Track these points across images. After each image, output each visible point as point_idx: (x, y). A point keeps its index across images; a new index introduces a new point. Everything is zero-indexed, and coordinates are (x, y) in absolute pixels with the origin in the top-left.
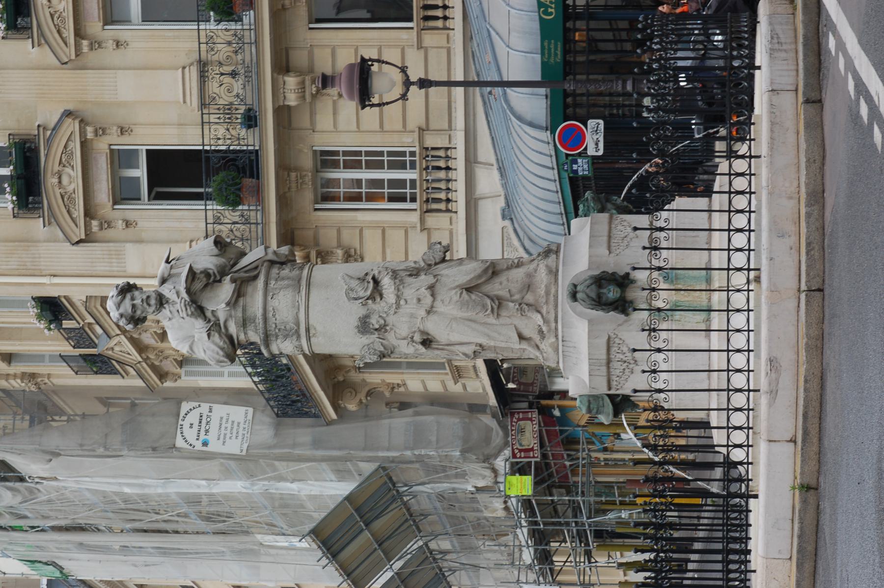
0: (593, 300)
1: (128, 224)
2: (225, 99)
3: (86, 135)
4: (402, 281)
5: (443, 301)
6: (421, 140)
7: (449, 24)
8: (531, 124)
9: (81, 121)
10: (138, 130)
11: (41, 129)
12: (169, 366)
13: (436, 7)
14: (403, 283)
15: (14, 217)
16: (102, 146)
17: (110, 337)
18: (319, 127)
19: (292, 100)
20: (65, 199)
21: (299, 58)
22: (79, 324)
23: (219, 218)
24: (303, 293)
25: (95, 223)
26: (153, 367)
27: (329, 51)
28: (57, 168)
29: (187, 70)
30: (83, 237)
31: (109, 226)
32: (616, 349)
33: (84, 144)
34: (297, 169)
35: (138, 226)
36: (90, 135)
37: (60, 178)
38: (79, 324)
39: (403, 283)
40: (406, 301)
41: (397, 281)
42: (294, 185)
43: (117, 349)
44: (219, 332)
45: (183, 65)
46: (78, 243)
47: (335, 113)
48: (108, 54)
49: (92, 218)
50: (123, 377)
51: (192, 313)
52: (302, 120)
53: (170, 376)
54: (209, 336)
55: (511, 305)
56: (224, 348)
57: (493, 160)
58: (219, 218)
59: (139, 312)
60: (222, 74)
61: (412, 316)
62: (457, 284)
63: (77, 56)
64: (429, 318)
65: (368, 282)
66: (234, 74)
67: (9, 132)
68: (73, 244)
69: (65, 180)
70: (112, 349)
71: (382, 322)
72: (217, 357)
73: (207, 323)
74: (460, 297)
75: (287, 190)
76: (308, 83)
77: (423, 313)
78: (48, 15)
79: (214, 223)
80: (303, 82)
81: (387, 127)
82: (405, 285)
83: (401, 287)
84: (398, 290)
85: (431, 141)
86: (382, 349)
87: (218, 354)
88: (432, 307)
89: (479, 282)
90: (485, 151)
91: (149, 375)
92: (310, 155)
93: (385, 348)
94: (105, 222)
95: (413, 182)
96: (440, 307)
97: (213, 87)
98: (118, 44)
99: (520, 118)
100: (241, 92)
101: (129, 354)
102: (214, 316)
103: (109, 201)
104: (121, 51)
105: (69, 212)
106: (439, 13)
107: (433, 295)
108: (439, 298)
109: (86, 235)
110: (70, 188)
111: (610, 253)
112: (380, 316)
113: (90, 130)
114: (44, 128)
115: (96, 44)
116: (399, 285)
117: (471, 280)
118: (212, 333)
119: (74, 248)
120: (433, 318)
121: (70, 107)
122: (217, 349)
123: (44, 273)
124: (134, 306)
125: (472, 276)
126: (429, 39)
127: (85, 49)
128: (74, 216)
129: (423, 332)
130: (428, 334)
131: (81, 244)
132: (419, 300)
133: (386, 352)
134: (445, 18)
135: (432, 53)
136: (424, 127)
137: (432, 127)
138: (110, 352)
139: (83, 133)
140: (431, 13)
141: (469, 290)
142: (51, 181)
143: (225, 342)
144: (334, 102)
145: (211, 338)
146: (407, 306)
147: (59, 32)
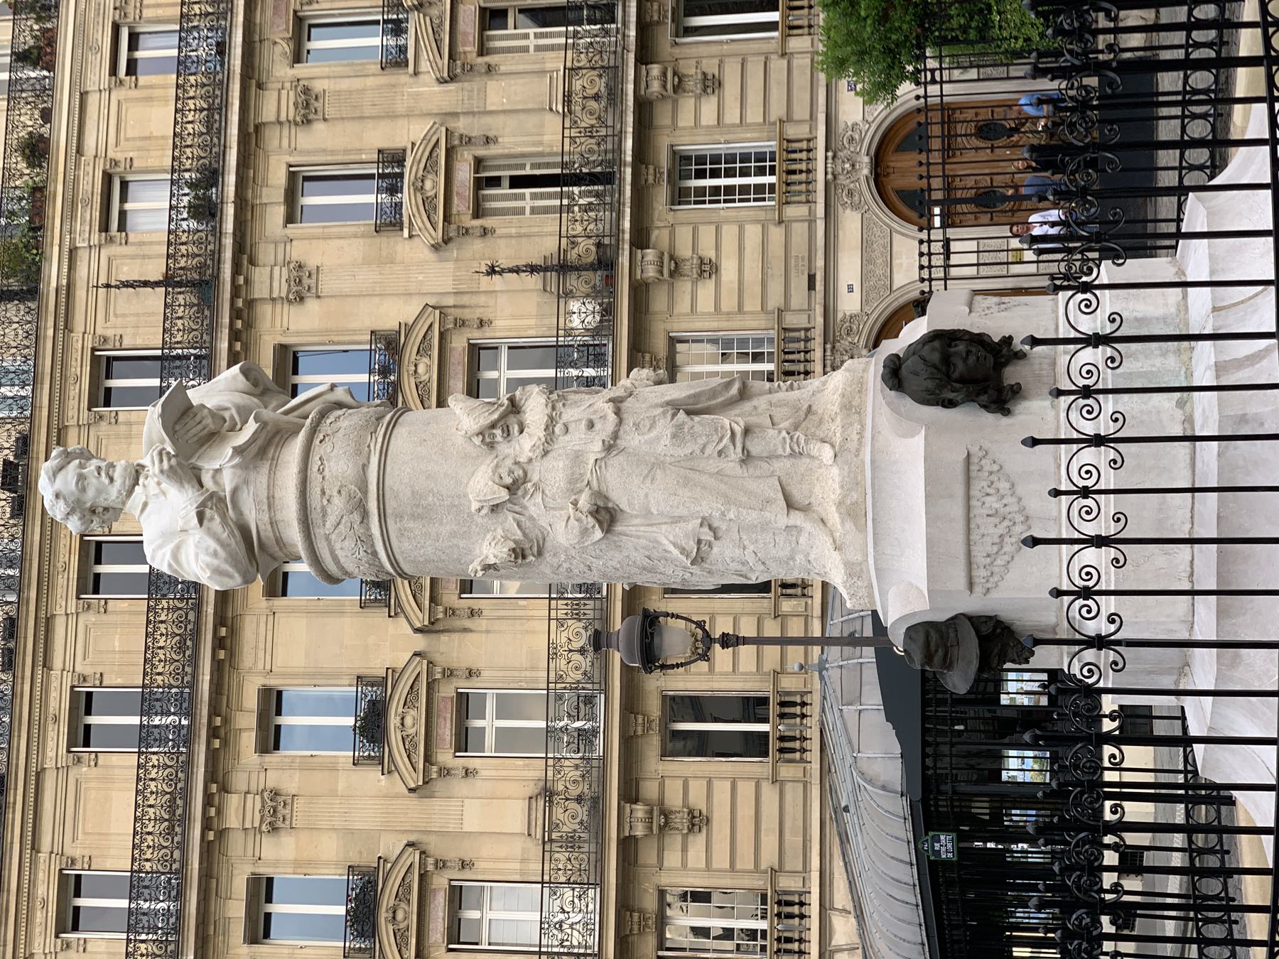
0: (934, 366)
2: (569, 826)
3: (426, 866)
5: (637, 425)
6: (773, 882)
7: (807, 756)
8: (884, 788)
9: (423, 853)
10: (480, 865)
11: (382, 861)
13: (793, 739)
16: (440, 882)
18: (666, 864)
19: (639, 831)
21: (650, 789)
27: (680, 783)
28: (392, 903)
29: (533, 801)
32: (985, 484)
33: (423, 877)
34: (641, 911)
36: (430, 868)
37: (394, 912)
42: (636, 927)
44: (224, 517)
45: (529, 794)
47: (684, 850)
48: (459, 786)
51: (171, 467)
52: (648, 855)
54: (201, 517)
55: (772, 432)
56: (229, 545)
57: (850, 907)
59: (91, 493)
60: (567, 799)
61: (577, 457)
62: (668, 398)
63: (425, 783)
64: (610, 462)
66: (579, 799)
67: (350, 864)
69: (400, 915)
72: (216, 562)
73: (202, 494)
74: (672, 419)
75: (628, 932)
76: (656, 813)
78: (400, 738)
80: (651, 812)
81: (739, 866)
84: (554, 408)
85: (786, 883)
87: (215, 554)
88: (615, 436)
90: (841, 897)
92: (656, 894)
93: (525, 534)
95: (764, 932)
96: (631, 439)
97: (559, 813)
98: (467, 773)
99: (870, 782)
100: (585, 818)
102: (216, 482)
104: (470, 780)
105: (399, 951)
106: (797, 745)
107: (618, 412)
108: (629, 421)
110: (402, 926)
111: (970, 311)
112: (516, 463)
113: (431, 861)
114: (385, 861)
115: (445, 772)
118: (208, 512)
120: (616, 461)
121: (412, 838)
122: (213, 545)
124: (81, 478)
126: (786, 771)
127: (434, 776)
129: (599, 495)
130: (607, 498)
132: (591, 425)
133: (527, 546)
134: (803, 750)
135: (788, 786)
136: (777, 868)
137: (788, 867)
139: (422, 864)
140: (787, 745)
141: (689, 413)
142: (383, 915)
143: (232, 532)
144: (685, 837)
145: (205, 522)
146: (567, 438)
147: (409, 756)
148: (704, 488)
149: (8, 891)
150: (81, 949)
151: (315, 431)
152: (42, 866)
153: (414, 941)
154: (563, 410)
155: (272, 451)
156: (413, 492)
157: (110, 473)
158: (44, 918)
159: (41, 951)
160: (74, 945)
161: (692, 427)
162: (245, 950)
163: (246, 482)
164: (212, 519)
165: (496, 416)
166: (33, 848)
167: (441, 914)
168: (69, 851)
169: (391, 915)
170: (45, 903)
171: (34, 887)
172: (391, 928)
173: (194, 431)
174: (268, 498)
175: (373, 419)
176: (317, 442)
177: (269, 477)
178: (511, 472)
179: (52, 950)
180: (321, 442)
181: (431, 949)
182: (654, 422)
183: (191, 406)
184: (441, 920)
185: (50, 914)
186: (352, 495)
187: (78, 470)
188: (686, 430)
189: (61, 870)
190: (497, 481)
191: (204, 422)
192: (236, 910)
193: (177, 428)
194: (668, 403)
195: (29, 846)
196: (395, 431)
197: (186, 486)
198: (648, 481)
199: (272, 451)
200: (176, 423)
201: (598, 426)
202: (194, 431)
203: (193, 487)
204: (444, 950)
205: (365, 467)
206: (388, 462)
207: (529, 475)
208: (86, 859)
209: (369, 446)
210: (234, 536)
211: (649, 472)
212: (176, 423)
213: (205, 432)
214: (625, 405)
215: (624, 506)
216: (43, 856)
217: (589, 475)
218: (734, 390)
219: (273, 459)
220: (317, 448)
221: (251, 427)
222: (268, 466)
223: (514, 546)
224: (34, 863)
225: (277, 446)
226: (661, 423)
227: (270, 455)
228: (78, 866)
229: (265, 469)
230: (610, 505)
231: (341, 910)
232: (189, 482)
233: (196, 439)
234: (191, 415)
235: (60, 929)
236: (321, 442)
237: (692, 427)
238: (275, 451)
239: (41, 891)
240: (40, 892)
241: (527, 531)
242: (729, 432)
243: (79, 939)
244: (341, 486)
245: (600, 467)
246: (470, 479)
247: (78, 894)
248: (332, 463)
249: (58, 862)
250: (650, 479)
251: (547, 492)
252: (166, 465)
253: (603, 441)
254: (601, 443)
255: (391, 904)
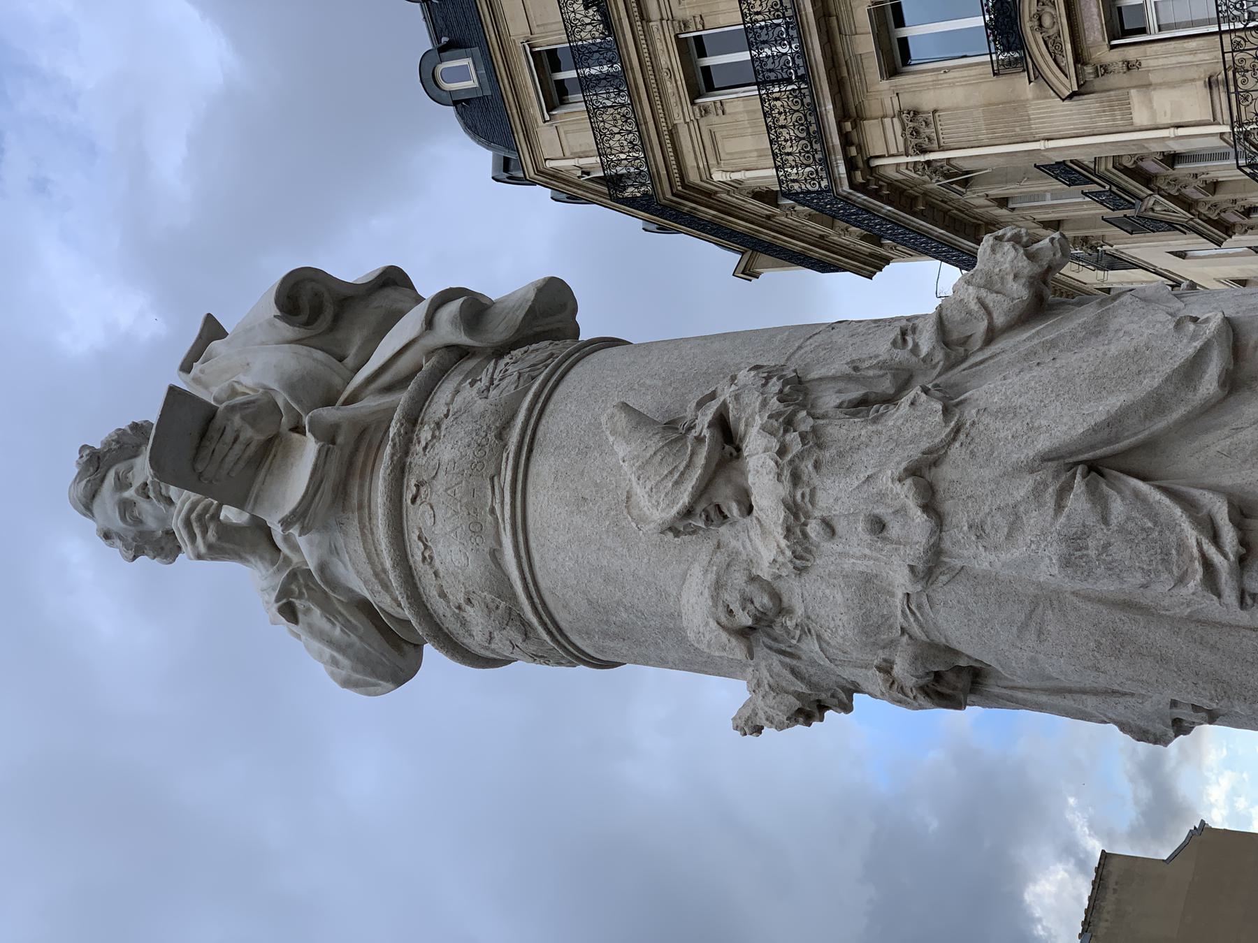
1: (1129, 66)
4: (815, 439)
5: (979, 529)
12: (1232, 218)
14: (820, 446)
15: (995, 74)
17: (1142, 200)
20: (1050, 45)
22: (1104, 187)
23: (1239, 43)
24: (508, 475)
25: (1089, 69)
26: (1209, 221)
28: (1034, 9)
30: (1076, 89)
31: (1106, 71)
35: (1143, 65)
37: (1040, 19)
38: (1104, 187)
39: (820, 446)
40: (829, 527)
41: (792, 437)
43: (1158, 208)
46: (1070, 97)
49: (1085, 64)
50: (1185, 233)
53: (1237, 229)
56: (350, 645)
58: (1239, 43)
62: (1043, 444)
65: (699, 440)
68: (1063, 100)
69: (1047, 21)
70: (1153, 210)
71: (763, 600)
74: (1059, 507)
77: (900, 580)
79: (1233, 51)
82: (827, 455)
83: (807, 467)
84: (796, 478)
86: (801, 687)
89: (1160, 424)
91: (1209, 230)
93: (810, 684)
94: (1101, 66)
101: (1174, 212)
103: (1104, 40)
107: (930, 505)
108: (959, 516)
109: (1079, 86)
110: (1052, 32)
112: (753, 579)
116: (801, 456)
117: (1115, 422)
118: (299, 604)
119: (1066, 103)
120: (948, 594)
123: (1037, 136)
125: (1114, 402)
128: (1063, 64)
131: (1076, 98)
132: (878, 526)
138: (1151, 213)
142: (1028, 25)
143: (347, 625)
145: (300, 616)
148: (1163, 660)
149: (632, 69)
150: (720, 112)
151: (403, 472)
152: (657, 36)
153: (1069, 46)
154: (816, 481)
155: (356, 489)
156: (590, 602)
157: (164, 492)
158: (676, 86)
159: (682, 120)
160: (712, 108)
161: (1106, 546)
162: (885, 84)
163: (334, 551)
164: (308, 611)
165: (685, 499)
166: (642, 19)
167: (1095, 10)
168: (679, 13)
169: (1036, 23)
170: (671, 71)
171: (656, 58)
172: (1039, 37)
173: (231, 458)
174: (376, 575)
175: (491, 436)
176: (408, 496)
177: (365, 542)
178: (747, 600)
179: (693, 118)
180: (414, 500)
181: (1091, 50)
182: (1018, 517)
183: (210, 414)
184: (1096, 17)
185: (679, 83)
186: (492, 606)
187: (117, 496)
188: (1092, 553)
189: (676, 36)
190: (723, 620)
191: (241, 438)
192: (865, 45)
193: (200, 467)
194: (1046, 458)
195: (638, 18)
196: (533, 470)
197: (252, 560)
198: (1031, 637)
199: (356, 489)
200: (195, 459)
201: (894, 530)
202: (231, 458)
203: (262, 558)
204: (1106, 48)
205: (495, 555)
206: (533, 544)
207: (785, 599)
208: (698, 19)
209: (492, 511)
210: (354, 629)
211: (1029, 616)
212: (195, 459)
213: (252, 448)
214: (946, 473)
215: (988, 658)
216: (654, 25)
217: (900, 619)
218: (1209, 384)
219: (361, 507)
220: (411, 515)
221: (310, 448)
222: (356, 522)
223: (798, 704)
224: (647, 33)
225: (362, 477)
226: (1035, 520)
227: (355, 502)
228: (692, 28)
229: (354, 529)
230: (963, 663)
231: (979, 22)
232: (253, 553)
233: (242, 464)
234: (216, 436)
235: (694, 94)
236: (414, 500)
237: (1106, 546)
238: (361, 487)
239: (664, 61)
240: (663, 63)
241: (815, 679)
242: (1197, 565)
243: (715, 102)
244: (467, 593)
245: (919, 607)
246: (680, 588)
247: (702, 53)
248: (440, 546)
249: (671, 28)
250: (1033, 628)
251: (826, 636)
252: (202, 549)
253: (912, 568)
254: (906, 571)
255: (1034, 10)
